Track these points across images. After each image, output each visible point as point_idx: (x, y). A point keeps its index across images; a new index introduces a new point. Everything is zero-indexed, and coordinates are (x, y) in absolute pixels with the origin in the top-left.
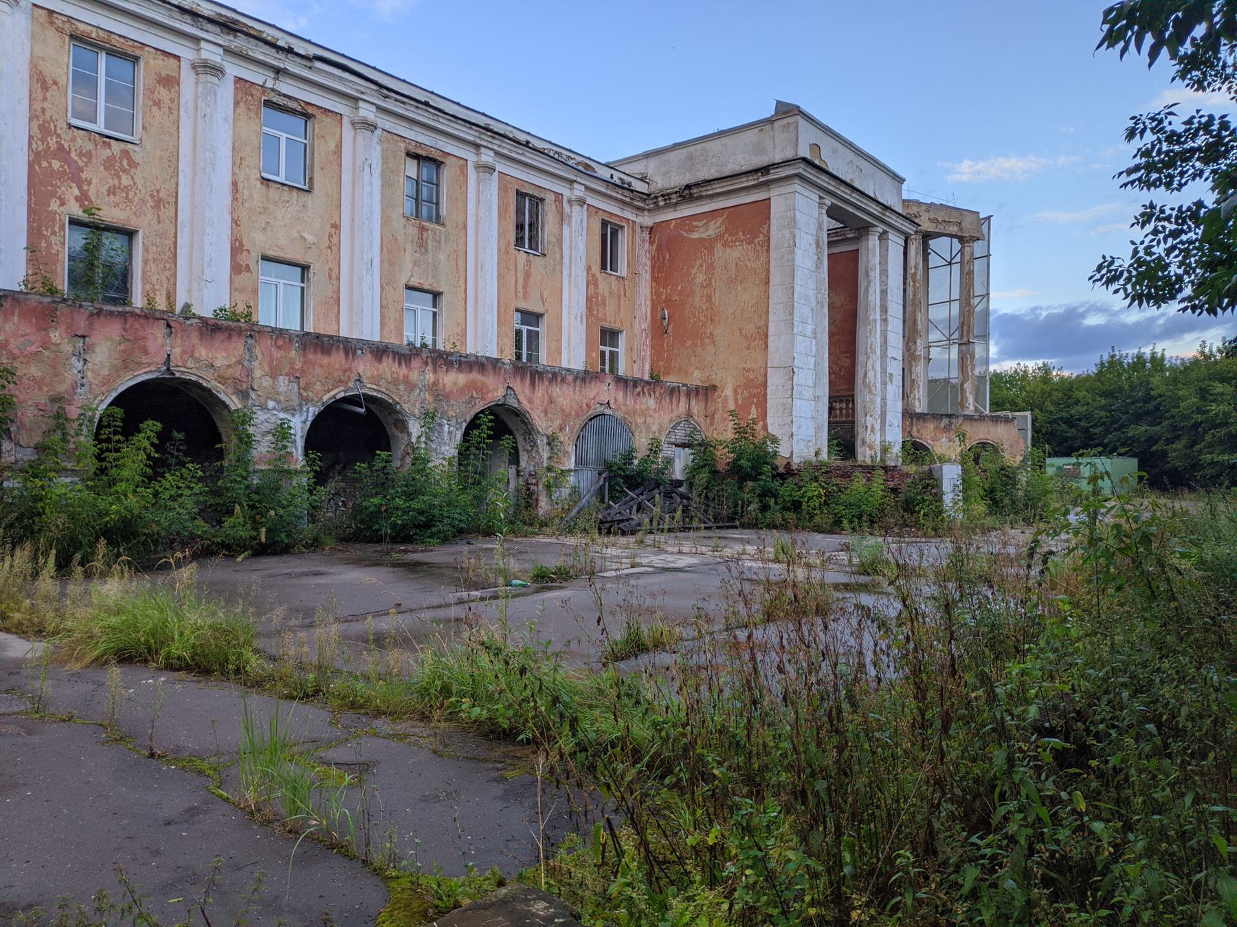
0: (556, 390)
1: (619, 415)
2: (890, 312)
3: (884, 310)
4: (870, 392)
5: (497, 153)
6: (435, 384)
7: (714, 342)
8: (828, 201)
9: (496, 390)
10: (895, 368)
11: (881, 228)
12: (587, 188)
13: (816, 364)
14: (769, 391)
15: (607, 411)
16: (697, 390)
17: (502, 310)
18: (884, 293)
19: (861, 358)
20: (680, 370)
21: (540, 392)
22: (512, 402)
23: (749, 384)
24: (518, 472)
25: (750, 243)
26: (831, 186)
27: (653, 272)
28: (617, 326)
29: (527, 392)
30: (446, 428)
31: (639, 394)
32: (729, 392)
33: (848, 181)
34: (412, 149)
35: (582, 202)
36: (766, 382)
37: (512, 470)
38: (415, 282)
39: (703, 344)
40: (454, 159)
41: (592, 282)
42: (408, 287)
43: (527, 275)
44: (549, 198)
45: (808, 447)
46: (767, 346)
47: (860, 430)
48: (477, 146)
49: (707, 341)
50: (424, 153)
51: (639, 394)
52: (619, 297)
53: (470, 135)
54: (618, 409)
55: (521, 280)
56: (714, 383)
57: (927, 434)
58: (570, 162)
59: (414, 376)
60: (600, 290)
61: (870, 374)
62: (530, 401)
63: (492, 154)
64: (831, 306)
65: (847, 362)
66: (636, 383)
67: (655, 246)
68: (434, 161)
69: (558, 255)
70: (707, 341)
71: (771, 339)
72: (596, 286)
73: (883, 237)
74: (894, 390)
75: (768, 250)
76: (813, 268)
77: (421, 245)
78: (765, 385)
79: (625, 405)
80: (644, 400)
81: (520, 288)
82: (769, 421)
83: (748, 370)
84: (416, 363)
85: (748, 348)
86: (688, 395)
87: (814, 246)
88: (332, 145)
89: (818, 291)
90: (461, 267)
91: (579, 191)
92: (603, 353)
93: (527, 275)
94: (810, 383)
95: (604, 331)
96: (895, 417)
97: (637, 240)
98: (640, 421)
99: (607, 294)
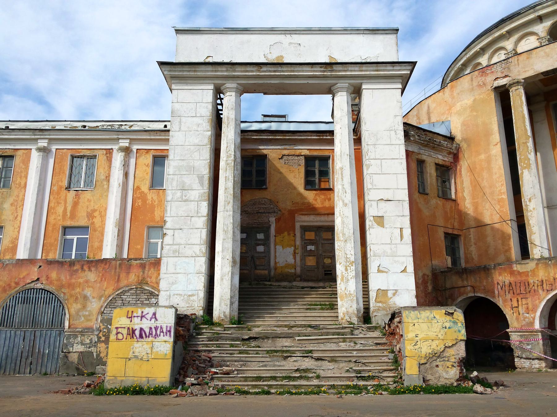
31: (77, 271)
44: (99, 154)
54: (51, 283)
55: (69, 209)
69: (106, 186)
79: (59, 280)
80: (82, 274)
81: (68, 214)
93: (76, 204)
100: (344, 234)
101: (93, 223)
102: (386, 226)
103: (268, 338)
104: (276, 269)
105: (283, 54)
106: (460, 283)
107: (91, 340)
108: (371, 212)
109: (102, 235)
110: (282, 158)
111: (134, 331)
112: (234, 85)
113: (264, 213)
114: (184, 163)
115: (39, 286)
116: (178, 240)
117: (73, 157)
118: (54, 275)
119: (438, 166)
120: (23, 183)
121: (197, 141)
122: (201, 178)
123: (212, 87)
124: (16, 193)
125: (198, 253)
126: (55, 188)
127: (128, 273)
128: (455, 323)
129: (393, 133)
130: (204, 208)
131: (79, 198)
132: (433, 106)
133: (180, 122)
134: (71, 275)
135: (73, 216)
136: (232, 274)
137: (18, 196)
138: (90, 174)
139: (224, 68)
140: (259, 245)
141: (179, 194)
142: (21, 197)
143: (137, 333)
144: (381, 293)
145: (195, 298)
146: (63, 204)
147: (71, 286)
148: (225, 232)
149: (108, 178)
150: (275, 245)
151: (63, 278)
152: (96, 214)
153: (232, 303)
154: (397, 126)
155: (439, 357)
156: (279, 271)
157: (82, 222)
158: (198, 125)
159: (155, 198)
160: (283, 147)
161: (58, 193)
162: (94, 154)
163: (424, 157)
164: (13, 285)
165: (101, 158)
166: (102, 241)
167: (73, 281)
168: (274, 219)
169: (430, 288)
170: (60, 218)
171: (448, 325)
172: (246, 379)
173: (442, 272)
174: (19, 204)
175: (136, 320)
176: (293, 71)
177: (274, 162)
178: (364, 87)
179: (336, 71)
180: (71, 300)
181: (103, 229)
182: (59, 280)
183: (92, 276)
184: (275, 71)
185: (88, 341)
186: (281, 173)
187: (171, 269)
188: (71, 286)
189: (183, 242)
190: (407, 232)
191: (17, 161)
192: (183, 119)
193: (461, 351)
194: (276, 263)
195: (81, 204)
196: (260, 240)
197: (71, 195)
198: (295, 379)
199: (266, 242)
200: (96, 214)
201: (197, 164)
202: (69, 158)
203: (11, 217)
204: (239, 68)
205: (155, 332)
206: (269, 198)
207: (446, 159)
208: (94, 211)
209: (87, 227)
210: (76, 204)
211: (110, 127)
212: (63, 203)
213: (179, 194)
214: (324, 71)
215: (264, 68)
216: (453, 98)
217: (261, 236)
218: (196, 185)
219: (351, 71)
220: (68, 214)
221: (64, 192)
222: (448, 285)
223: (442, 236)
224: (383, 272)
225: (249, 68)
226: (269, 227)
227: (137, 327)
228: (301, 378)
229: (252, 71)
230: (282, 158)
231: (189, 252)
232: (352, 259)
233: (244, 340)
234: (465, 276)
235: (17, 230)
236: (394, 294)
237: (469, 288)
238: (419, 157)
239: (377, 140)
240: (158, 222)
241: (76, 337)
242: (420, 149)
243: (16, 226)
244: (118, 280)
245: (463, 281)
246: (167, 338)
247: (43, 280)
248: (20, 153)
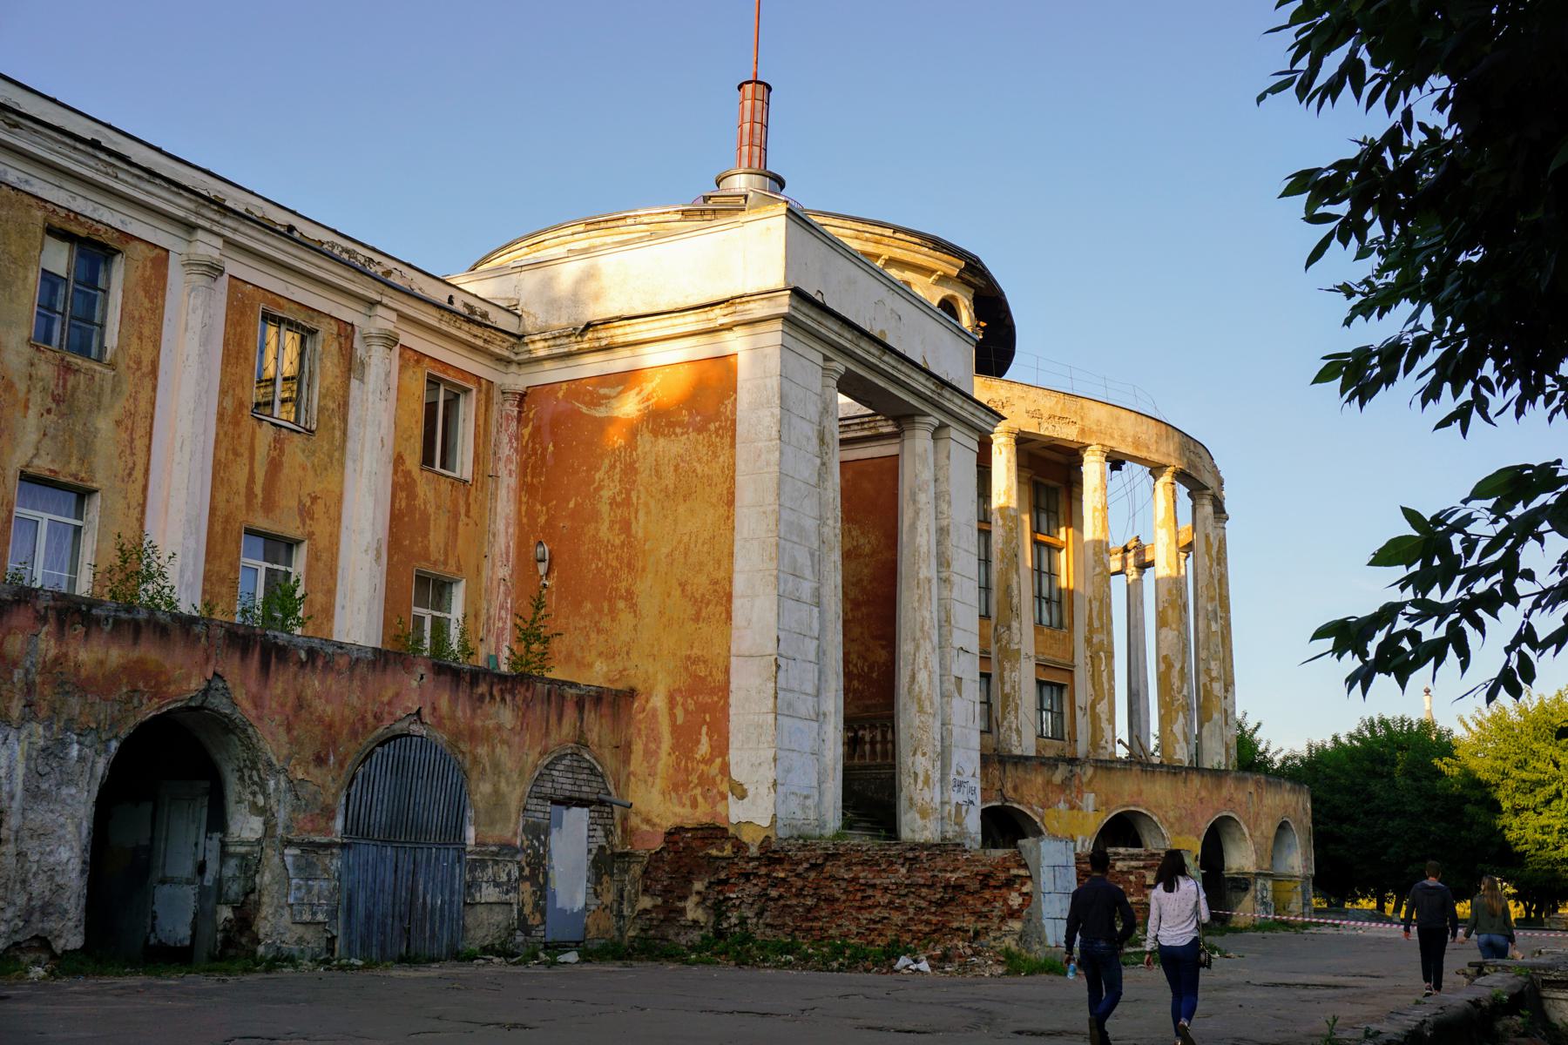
0: (314, 684)
1: (441, 737)
2: (956, 566)
3: (943, 562)
4: (921, 710)
5: (229, 243)
6: (57, 660)
7: (633, 607)
8: (840, 365)
9: (188, 677)
10: (968, 669)
11: (935, 418)
12: (402, 316)
13: (821, 652)
14: (733, 700)
15: (416, 729)
16: (600, 698)
17: (218, 528)
18: (942, 532)
19: (905, 647)
20: (569, 657)
21: (280, 684)
22: (218, 702)
23: (697, 686)
24: (224, 845)
25: (699, 431)
26: (846, 339)
27: (523, 474)
28: (449, 571)
30: (74, 751)
31: (481, 698)
32: (659, 701)
33: (876, 333)
34: (55, 221)
35: (391, 340)
36: (728, 682)
37: (214, 844)
38: (43, 465)
39: (612, 610)
40: (143, 246)
41: (402, 486)
42: (27, 478)
43: (275, 466)
44: (326, 330)
45: (804, 808)
46: (729, 617)
47: (905, 781)
48: (191, 228)
49: (621, 604)
50: (82, 232)
51: (481, 698)
52: (455, 516)
53: (180, 207)
54: (439, 724)
56: (634, 683)
57: (1029, 796)
58: (373, 269)
60: (419, 502)
61: (922, 676)
62: (257, 703)
63: (219, 243)
64: (847, 556)
65: (882, 655)
66: (476, 676)
67: (527, 431)
68: (103, 246)
69: (338, 434)
70: (621, 604)
71: (737, 603)
72: (412, 496)
73: (938, 432)
74: (965, 712)
75: (733, 445)
76: (814, 480)
77: (62, 401)
78: (725, 689)
79: (453, 718)
80: (493, 710)
81: (258, 489)
82: (734, 756)
83: (696, 661)
85: (697, 618)
86: (580, 704)
87: (815, 441)
89: (822, 520)
90: (140, 444)
91: (384, 321)
92: (419, 620)
93: (275, 466)
94: (810, 689)
95: (423, 580)
96: (967, 760)
97: (495, 415)
98: (482, 751)
99: (431, 510)
101: (311, 535)
107: (509, 875)
120: (146, 361)
124: (127, 388)
126: (229, 403)
131: (282, 451)
135: (269, 506)
137: (135, 398)
142: (143, 406)
146: (245, 460)
151: (459, 714)
159: (431, 496)
162: (313, 325)
164: (370, 719)
178: (953, 433)
185: (504, 878)
188: (473, 735)
200: (319, 509)
211: (345, 256)
212: (246, 454)
220: (258, 489)
221: (247, 421)
235: (135, 513)
240: (435, 563)
241: (484, 867)
244: (547, 734)
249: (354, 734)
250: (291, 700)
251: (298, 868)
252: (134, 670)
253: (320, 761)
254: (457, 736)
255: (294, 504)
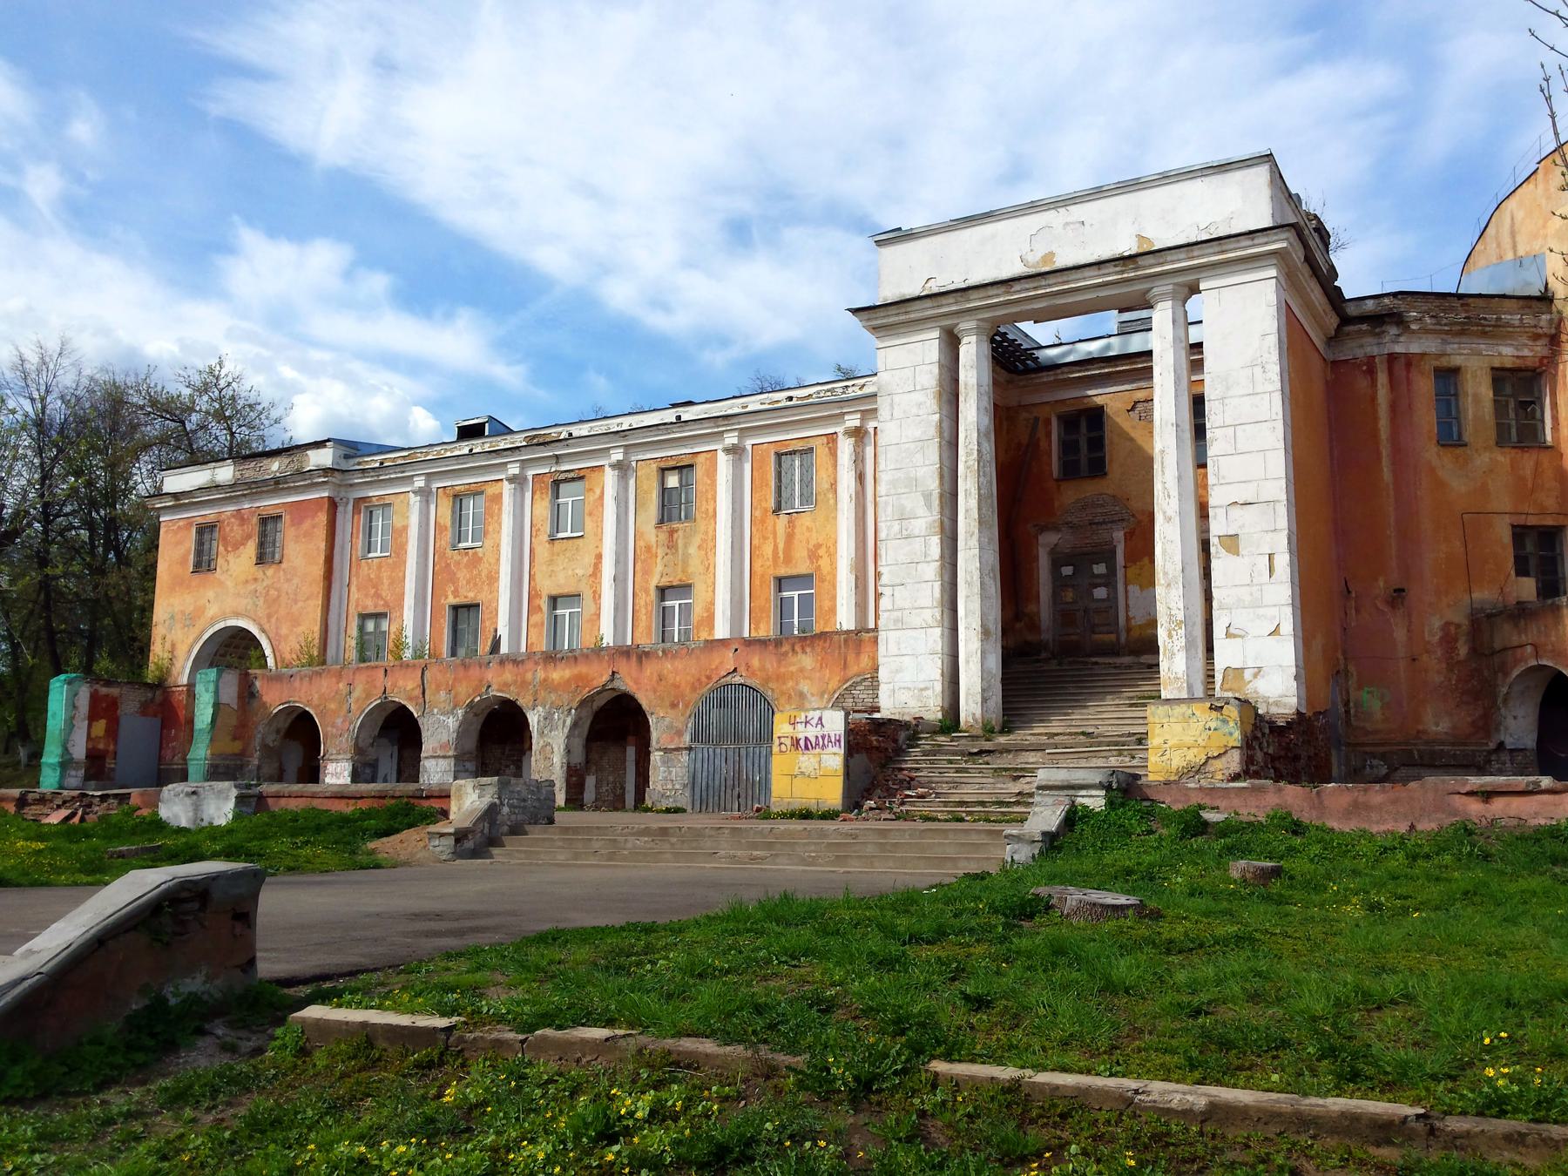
21: (650, 669)
29: (634, 673)
31: (785, 654)
34: (663, 465)
55: (781, 546)
59: (529, 676)
62: (637, 682)
77: (671, 545)
79: (763, 668)
84: (529, 665)
88: (598, 492)
93: (790, 537)
100: (1165, 574)
102: (1242, 551)
103: (1009, 751)
104: (1129, 630)
105: (1053, 248)
106: (1515, 640)
108: (1217, 528)
109: (834, 587)
110: (1133, 409)
111: (798, 741)
112: (972, 324)
113: (1104, 523)
114: (900, 474)
115: (737, 680)
116: (899, 603)
117: (779, 455)
118: (755, 662)
119: (1500, 376)
121: (918, 434)
122: (927, 497)
123: (936, 334)
124: (703, 528)
125: (930, 621)
126: (757, 513)
127: (858, 654)
128: (1225, 722)
129: (1258, 370)
130: (935, 546)
132: (1520, 215)
133: (892, 405)
134: (779, 662)
135: (788, 559)
136: (983, 652)
138: (807, 483)
139: (951, 299)
140: (1096, 586)
141: (896, 527)
143: (802, 743)
144: (1236, 673)
145: (930, 692)
147: (780, 678)
148: (969, 584)
149: (834, 486)
150: (1126, 585)
151: (768, 666)
152: (822, 552)
153: (984, 700)
154: (1266, 355)
155: (1197, 772)
156: (1135, 634)
157: (802, 568)
158: (919, 405)
160: (1134, 386)
161: (763, 522)
163: (1457, 361)
164: (704, 679)
165: (821, 452)
166: (834, 598)
167: (782, 670)
168: (1121, 534)
169: (1463, 650)
170: (770, 563)
171: (1213, 725)
172: (946, 804)
173: (1490, 616)
174: (709, 546)
175: (800, 727)
176: (1067, 282)
177: (1118, 420)
179: (1145, 267)
180: (783, 700)
181: (835, 576)
182: (763, 668)
183: (807, 660)
184: (1035, 288)
186: (1132, 440)
187: (893, 649)
188: (780, 678)
189: (907, 605)
190: (1283, 561)
191: (699, 472)
192: (896, 399)
193: (1234, 762)
194: (1128, 619)
195: (798, 536)
196: (1099, 576)
197: (783, 520)
198: (1008, 804)
199: (1109, 580)
200: (822, 552)
201: (921, 472)
202: (773, 458)
203: (701, 569)
204: (974, 295)
205: (821, 743)
206: (1110, 492)
207: (1526, 352)
208: (818, 546)
209: (811, 576)
210: (790, 537)
213: (896, 527)
214: (1122, 272)
215: (1017, 287)
216: (1548, 198)
217: (1100, 569)
218: (921, 510)
219: (1173, 262)
222: (1497, 645)
223: (1506, 536)
224: (1235, 636)
225: (991, 291)
226: (1113, 552)
227: (801, 736)
228: (1018, 803)
229: (998, 296)
230: (1133, 409)
231: (917, 622)
232: (1181, 616)
233: (971, 754)
234: (1522, 622)
236: (1255, 676)
237: (1529, 649)
238: (1444, 362)
239: (1228, 388)
242: (1444, 342)
243: (709, 582)
244: (845, 666)
245: (1519, 634)
246: (836, 749)
247: (742, 670)
248: (701, 458)
249: (694, 689)
250: (655, 677)
251: (664, 763)
252: (579, 678)
253: (674, 706)
254: (767, 680)
255: (805, 553)
